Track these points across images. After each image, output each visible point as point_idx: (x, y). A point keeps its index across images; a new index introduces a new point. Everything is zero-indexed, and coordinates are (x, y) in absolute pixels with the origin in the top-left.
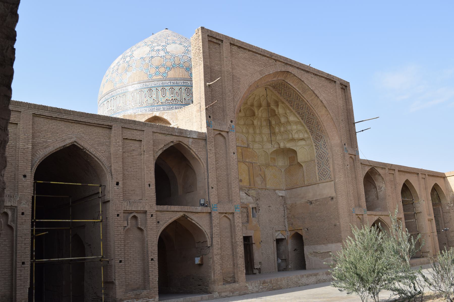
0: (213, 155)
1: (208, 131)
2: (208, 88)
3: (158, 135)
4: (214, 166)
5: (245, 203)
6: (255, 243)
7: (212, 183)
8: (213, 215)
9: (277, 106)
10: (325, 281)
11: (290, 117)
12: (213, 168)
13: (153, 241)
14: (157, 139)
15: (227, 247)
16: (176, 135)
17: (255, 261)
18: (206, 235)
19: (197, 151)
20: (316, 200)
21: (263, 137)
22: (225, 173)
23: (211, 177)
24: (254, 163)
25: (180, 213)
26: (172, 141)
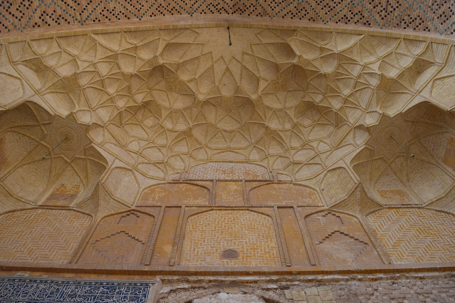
9: (290, 52)
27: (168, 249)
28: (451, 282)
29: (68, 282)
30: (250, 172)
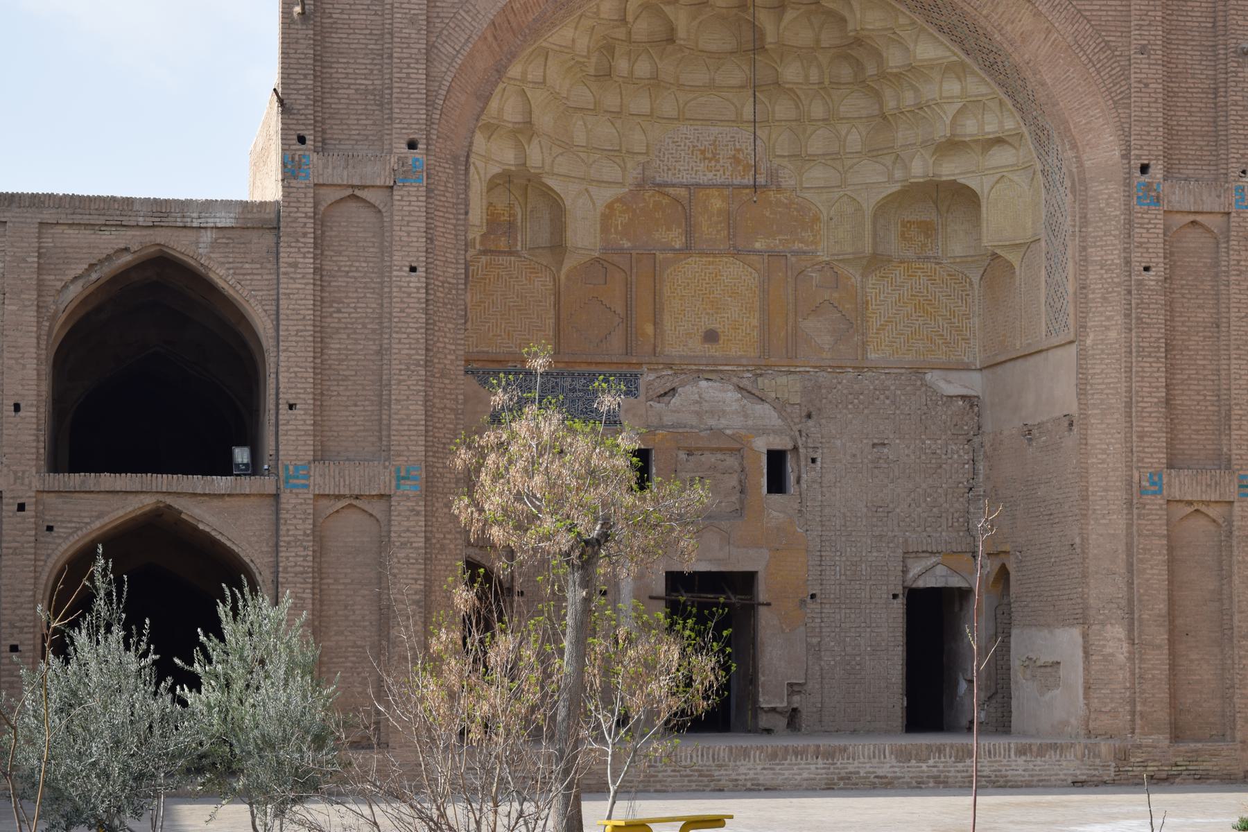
0: (306, 284)
1: (286, 194)
2: (300, 27)
3: (63, 233)
4: (305, 325)
5: (728, 432)
6: (768, 604)
7: (290, 388)
8: (288, 503)
10: (890, 783)
11: (916, 42)
12: (302, 331)
13: (21, 591)
14: (59, 245)
15: (359, 618)
16: (140, 224)
17: (762, 679)
18: (257, 574)
19: (235, 274)
20: (1040, 425)
21: (843, 133)
22: (374, 347)
23: (289, 368)
24: (795, 253)
25: (142, 497)
26: (122, 246)
27: (649, 329)
28: (913, 378)
29: (563, 374)
30: (741, 156)
